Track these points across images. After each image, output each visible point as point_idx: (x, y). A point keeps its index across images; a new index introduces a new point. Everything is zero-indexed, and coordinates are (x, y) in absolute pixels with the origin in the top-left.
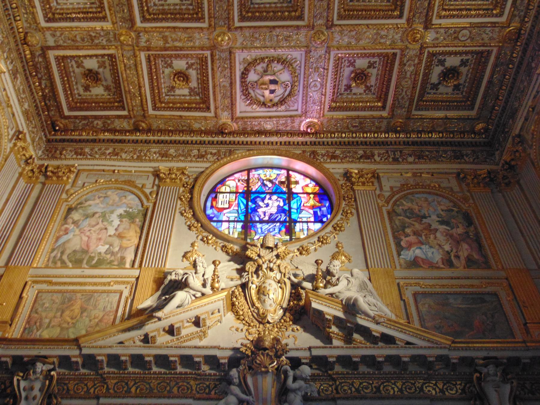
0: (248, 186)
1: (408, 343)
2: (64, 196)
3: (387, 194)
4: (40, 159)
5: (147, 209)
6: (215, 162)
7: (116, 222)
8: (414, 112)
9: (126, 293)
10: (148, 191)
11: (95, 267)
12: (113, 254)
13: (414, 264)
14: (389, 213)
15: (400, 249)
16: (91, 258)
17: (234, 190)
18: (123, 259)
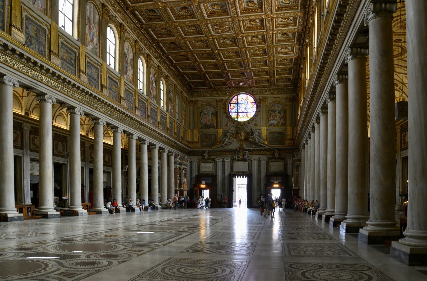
0: (238, 101)
1: (264, 146)
2: (198, 109)
3: (268, 105)
4: (190, 97)
5: (216, 112)
6: (229, 96)
7: (211, 116)
8: (276, 84)
9: (216, 135)
10: (216, 106)
11: (209, 128)
12: (212, 125)
13: (271, 125)
14: (268, 111)
15: (269, 121)
16: (208, 126)
17: (235, 103)
18: (214, 126)
